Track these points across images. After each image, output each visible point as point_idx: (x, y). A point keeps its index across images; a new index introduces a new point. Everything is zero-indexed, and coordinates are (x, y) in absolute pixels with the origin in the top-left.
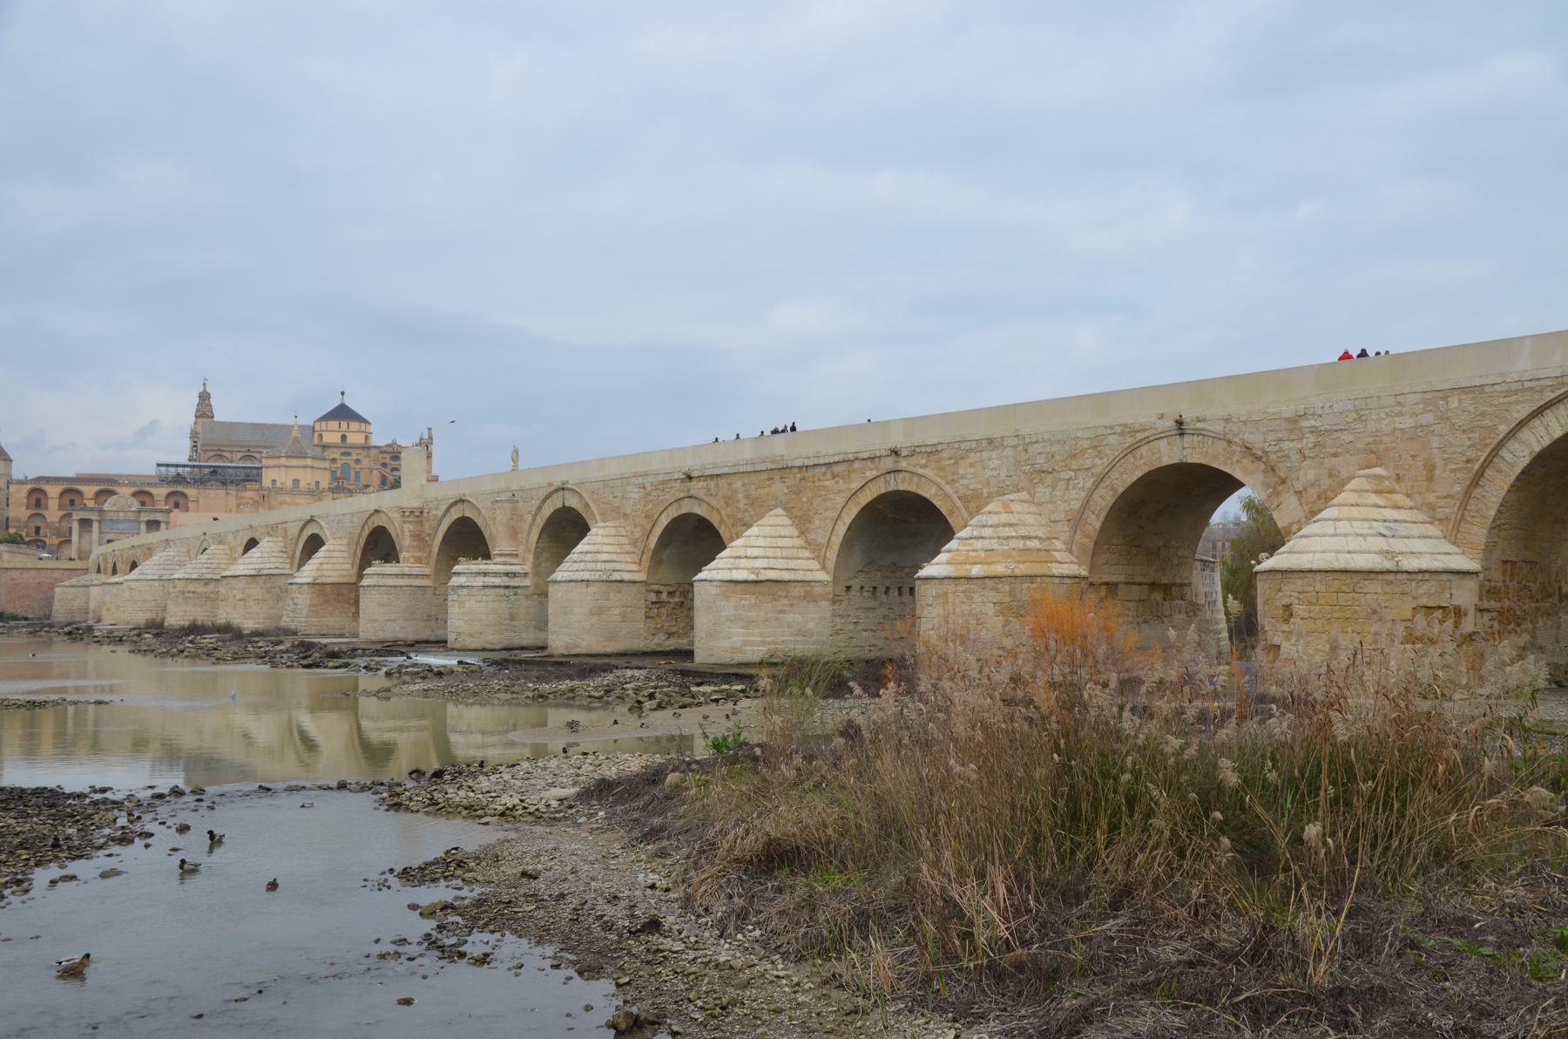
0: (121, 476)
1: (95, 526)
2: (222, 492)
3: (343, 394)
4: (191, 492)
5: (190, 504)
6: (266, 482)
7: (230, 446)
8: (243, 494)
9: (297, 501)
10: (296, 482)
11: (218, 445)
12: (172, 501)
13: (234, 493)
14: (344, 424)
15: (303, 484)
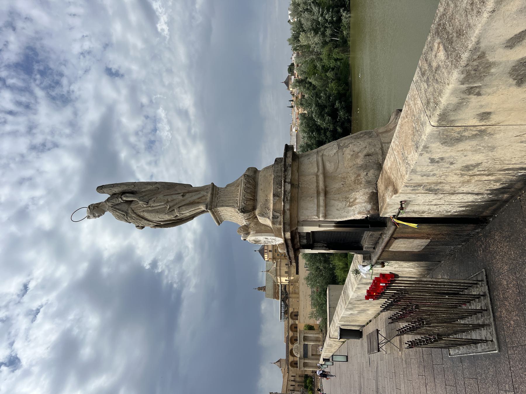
0: (285, 335)
1: (306, 361)
2: (290, 299)
3: (255, 251)
4: (291, 310)
5: (295, 311)
6: (286, 283)
7: (274, 289)
8: (291, 292)
9: (293, 272)
10: (286, 272)
11: (274, 293)
12: (295, 317)
13: (290, 295)
14: (266, 251)
15: (287, 270)
